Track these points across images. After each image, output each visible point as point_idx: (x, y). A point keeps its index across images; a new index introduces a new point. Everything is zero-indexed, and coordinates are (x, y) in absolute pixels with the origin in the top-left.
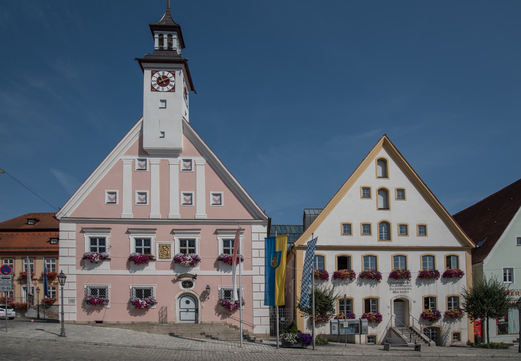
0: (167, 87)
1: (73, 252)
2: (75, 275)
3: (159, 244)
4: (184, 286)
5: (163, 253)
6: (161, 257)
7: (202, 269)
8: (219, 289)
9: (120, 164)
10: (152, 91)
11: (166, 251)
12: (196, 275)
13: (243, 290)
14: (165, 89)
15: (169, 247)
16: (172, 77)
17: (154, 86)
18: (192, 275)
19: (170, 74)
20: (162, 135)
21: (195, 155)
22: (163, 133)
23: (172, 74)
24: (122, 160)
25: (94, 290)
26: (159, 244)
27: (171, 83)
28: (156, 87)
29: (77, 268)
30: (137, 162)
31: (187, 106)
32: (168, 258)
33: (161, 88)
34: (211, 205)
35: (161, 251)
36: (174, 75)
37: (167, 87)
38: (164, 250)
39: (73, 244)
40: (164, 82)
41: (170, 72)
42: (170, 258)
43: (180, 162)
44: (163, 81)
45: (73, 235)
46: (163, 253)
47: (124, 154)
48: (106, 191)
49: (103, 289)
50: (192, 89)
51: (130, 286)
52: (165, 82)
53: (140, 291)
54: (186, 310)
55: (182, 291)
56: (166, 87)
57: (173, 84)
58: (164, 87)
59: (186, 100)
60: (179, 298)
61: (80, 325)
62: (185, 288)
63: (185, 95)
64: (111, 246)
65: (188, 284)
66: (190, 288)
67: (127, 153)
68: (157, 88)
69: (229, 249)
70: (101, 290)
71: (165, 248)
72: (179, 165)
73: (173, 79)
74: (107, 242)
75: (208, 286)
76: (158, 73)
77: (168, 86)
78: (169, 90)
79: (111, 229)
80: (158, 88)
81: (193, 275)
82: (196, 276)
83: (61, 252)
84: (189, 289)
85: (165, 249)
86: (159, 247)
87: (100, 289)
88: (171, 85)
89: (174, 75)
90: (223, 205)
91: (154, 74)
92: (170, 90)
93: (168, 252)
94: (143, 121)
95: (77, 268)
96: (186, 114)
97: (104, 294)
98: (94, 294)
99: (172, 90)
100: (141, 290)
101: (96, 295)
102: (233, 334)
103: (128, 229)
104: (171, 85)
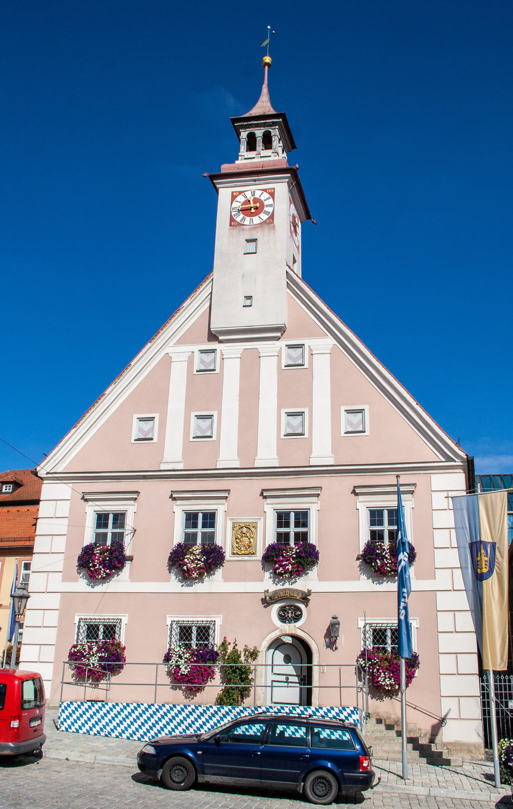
0: (259, 217)
1: (60, 544)
2: (60, 594)
3: (233, 523)
4: (283, 619)
5: (241, 541)
6: (235, 552)
7: (321, 578)
8: (361, 624)
9: (167, 360)
10: (231, 225)
11: (247, 537)
12: (309, 592)
13: (414, 627)
14: (256, 220)
15: (253, 529)
16: (269, 198)
17: (235, 218)
18: (301, 591)
19: (265, 194)
20: (248, 302)
21: (311, 335)
22: (249, 298)
23: (269, 193)
24: (170, 355)
25: (94, 629)
26: (233, 523)
27: (266, 209)
28: (238, 219)
29: (64, 580)
30: (197, 356)
31: (298, 248)
32: (250, 553)
33: (248, 219)
34: (343, 434)
35: (236, 539)
36: (272, 195)
37: (259, 217)
38: (242, 536)
39: (62, 526)
40: (252, 209)
41: (265, 190)
42: (254, 554)
43: (280, 351)
44: (252, 207)
45: (64, 509)
46: (241, 541)
47: (175, 344)
48: (136, 416)
49: (110, 626)
50: (309, 217)
51: (168, 618)
52: (254, 209)
53: (187, 631)
54: (283, 678)
55: (278, 630)
56: (257, 217)
57: (270, 210)
58: (253, 218)
59: (296, 236)
60: (269, 648)
61: (54, 710)
62: (285, 622)
63: (292, 227)
64: (136, 530)
65: (292, 613)
66: (295, 622)
67: (180, 342)
68: (241, 221)
69: (382, 531)
70: (107, 629)
71: (245, 530)
72: (279, 356)
73: (271, 201)
74: (129, 522)
75: (336, 618)
76: (243, 194)
77: (262, 215)
78: (262, 221)
79: (139, 493)
80: (243, 219)
81: (303, 593)
82: (309, 595)
83: (39, 545)
84: (292, 625)
85: (244, 534)
86: (234, 527)
87: (105, 626)
88: (267, 213)
89: (272, 195)
90: (367, 433)
91: (236, 196)
92: (266, 221)
93: (252, 540)
94: (213, 279)
95: (64, 580)
96: (295, 261)
97: (111, 636)
98: (93, 636)
99: (268, 221)
100: (190, 628)
101: (95, 639)
102: (390, 740)
103: (171, 491)
104: (267, 213)
